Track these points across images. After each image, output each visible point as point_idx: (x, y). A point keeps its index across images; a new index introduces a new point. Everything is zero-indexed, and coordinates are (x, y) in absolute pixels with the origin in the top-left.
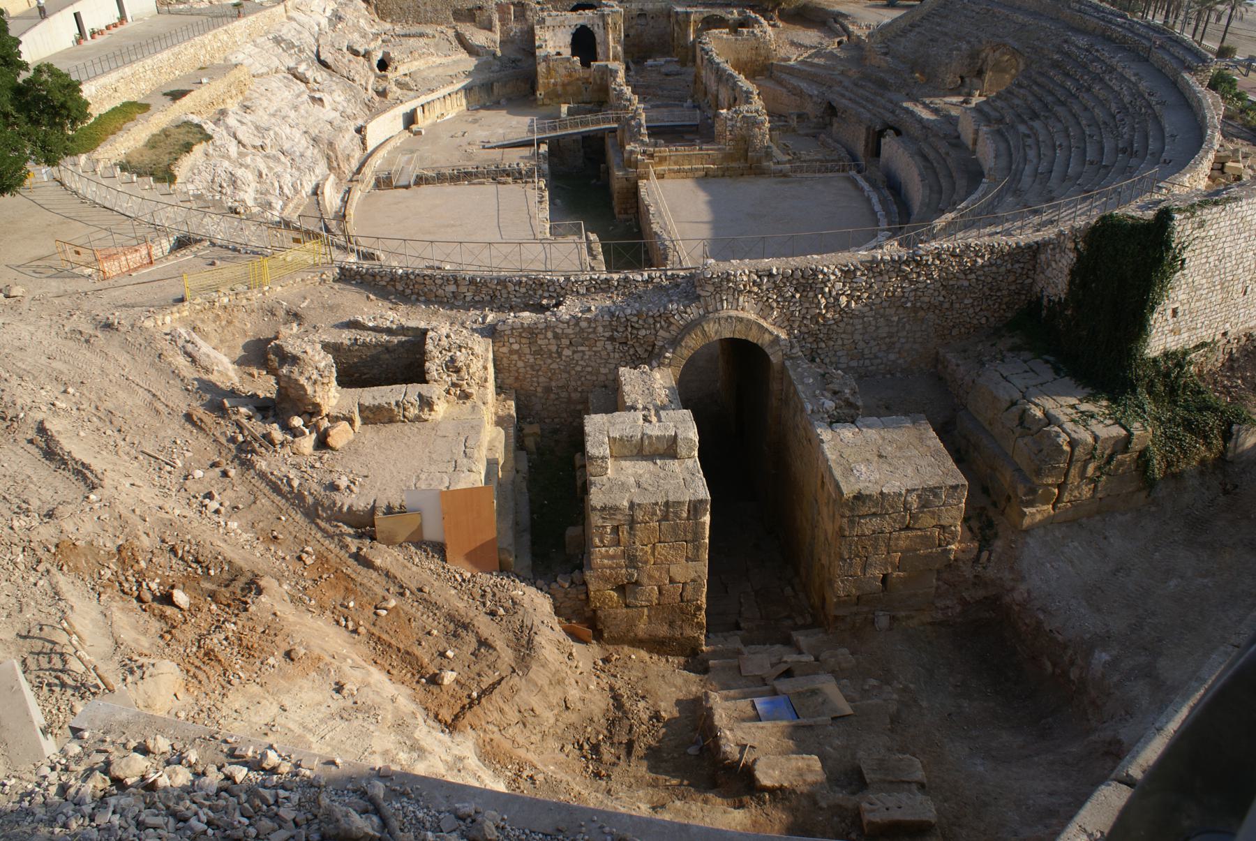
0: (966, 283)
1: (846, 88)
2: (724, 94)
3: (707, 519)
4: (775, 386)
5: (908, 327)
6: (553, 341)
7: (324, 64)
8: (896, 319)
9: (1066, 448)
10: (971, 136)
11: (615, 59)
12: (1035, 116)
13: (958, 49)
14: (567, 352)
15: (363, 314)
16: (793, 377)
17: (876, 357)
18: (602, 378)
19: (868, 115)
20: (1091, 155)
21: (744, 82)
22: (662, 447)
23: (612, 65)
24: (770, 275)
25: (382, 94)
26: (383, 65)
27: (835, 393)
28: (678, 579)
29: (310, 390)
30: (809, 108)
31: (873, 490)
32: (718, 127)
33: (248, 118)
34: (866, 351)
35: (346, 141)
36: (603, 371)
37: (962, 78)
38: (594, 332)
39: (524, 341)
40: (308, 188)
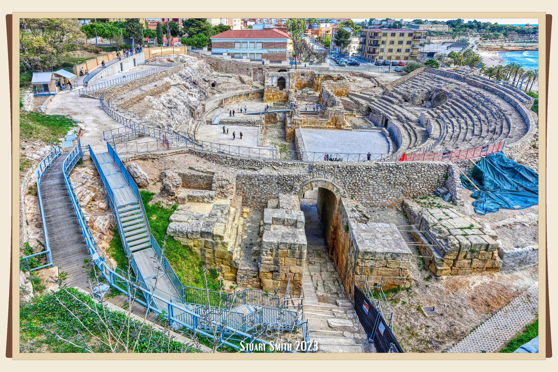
0: (416, 177)
1: (376, 103)
5: (391, 191)
8: (386, 187)
13: (422, 91)
16: (344, 204)
17: (377, 200)
18: (273, 196)
19: (384, 112)
20: (476, 132)
27: (360, 211)
34: (374, 198)
36: (274, 193)
37: (422, 101)
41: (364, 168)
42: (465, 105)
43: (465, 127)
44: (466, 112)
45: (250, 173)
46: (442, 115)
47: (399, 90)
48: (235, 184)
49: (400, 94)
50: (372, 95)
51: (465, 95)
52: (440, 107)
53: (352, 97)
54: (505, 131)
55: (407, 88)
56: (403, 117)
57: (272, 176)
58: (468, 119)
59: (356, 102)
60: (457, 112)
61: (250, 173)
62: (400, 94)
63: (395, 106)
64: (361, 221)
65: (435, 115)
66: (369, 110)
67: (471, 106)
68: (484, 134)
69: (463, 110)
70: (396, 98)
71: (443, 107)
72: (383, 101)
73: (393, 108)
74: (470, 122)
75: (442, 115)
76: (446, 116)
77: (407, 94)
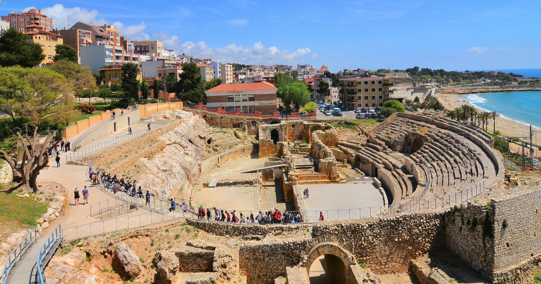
1: (364, 151)
6: (261, 254)
10: (410, 168)
12: (434, 160)
13: (401, 136)
14: (267, 259)
20: (457, 175)
21: (328, 149)
25: (209, 152)
26: (209, 142)
33: (162, 160)
38: (277, 250)
39: (251, 253)
41: (367, 225)
42: (440, 148)
43: (446, 171)
44: (443, 155)
45: (254, 243)
46: (423, 159)
47: (381, 136)
48: (238, 260)
49: (383, 140)
50: (358, 144)
51: (437, 138)
52: (419, 151)
53: (341, 146)
54: (480, 171)
55: (388, 134)
56: (390, 164)
58: (447, 162)
59: (346, 152)
60: (436, 155)
62: (383, 140)
63: (381, 153)
66: (358, 158)
67: (445, 148)
69: (440, 153)
70: (380, 145)
71: (422, 151)
72: (369, 148)
73: (379, 155)
74: (448, 165)
75: (423, 159)
76: (427, 160)
77: (389, 139)
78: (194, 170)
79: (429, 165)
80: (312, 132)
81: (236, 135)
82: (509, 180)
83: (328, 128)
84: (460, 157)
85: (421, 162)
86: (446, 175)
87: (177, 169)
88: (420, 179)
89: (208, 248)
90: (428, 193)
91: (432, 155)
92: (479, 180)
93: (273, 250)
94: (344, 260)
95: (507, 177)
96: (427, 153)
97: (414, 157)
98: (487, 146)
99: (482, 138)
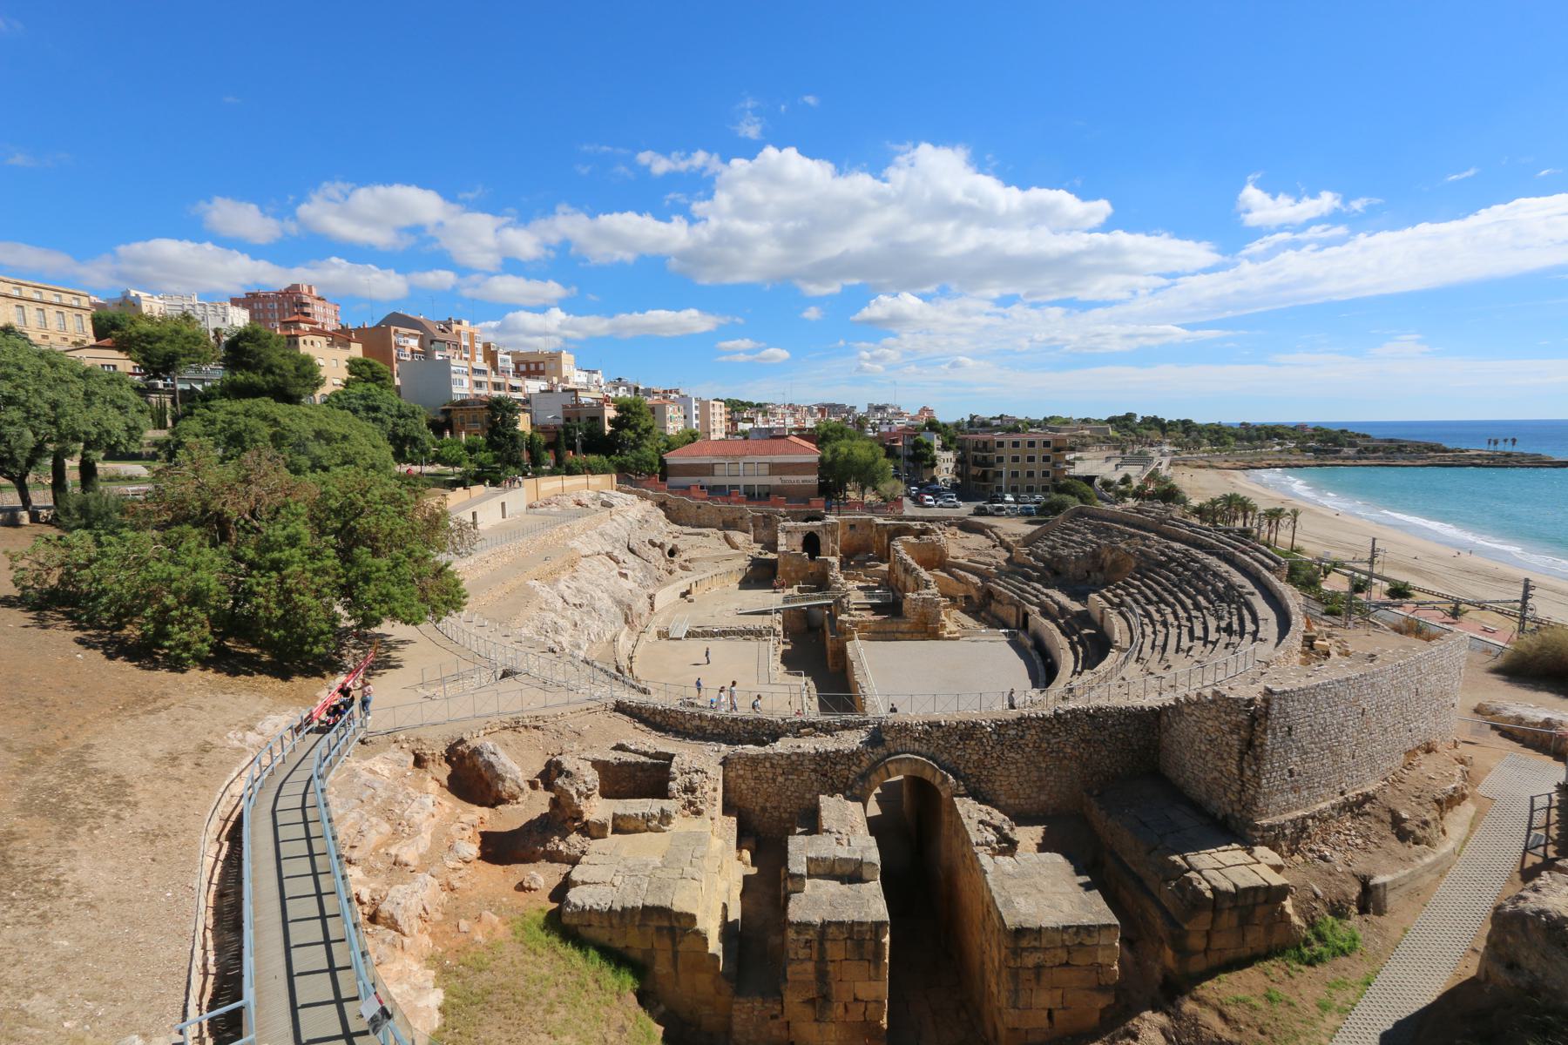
2: (910, 582)
3: (887, 939)
4: (945, 818)
7: (632, 551)
9: (1209, 894)
11: (833, 554)
12: (1150, 602)
14: (780, 779)
15: (628, 737)
20: (1199, 632)
21: (925, 575)
22: (849, 869)
23: (833, 559)
24: (940, 726)
25: (671, 572)
26: (672, 553)
28: (861, 995)
29: (576, 799)
30: (973, 592)
31: (1031, 923)
32: (906, 605)
33: (573, 584)
35: (641, 605)
40: (609, 636)
44: (1171, 593)
54: (1250, 627)
57: (803, 754)
58: (1178, 607)
60: (1156, 593)
61: (751, 749)
64: (1002, 852)
65: (1116, 600)
68: (1212, 636)
69: (1165, 589)
78: (640, 604)
79: (1139, 611)
80: (891, 538)
81: (726, 538)
82: (1311, 647)
83: (925, 532)
84: (1207, 598)
85: (1122, 603)
86: (1173, 632)
87: (605, 603)
88: (1117, 637)
89: (658, 755)
90: (1132, 664)
91: (1149, 593)
92: (1246, 644)
93: (794, 763)
94: (940, 788)
95: (1309, 641)
96: (1138, 588)
97: (1109, 595)
98: (1272, 578)
99: (1262, 563)
